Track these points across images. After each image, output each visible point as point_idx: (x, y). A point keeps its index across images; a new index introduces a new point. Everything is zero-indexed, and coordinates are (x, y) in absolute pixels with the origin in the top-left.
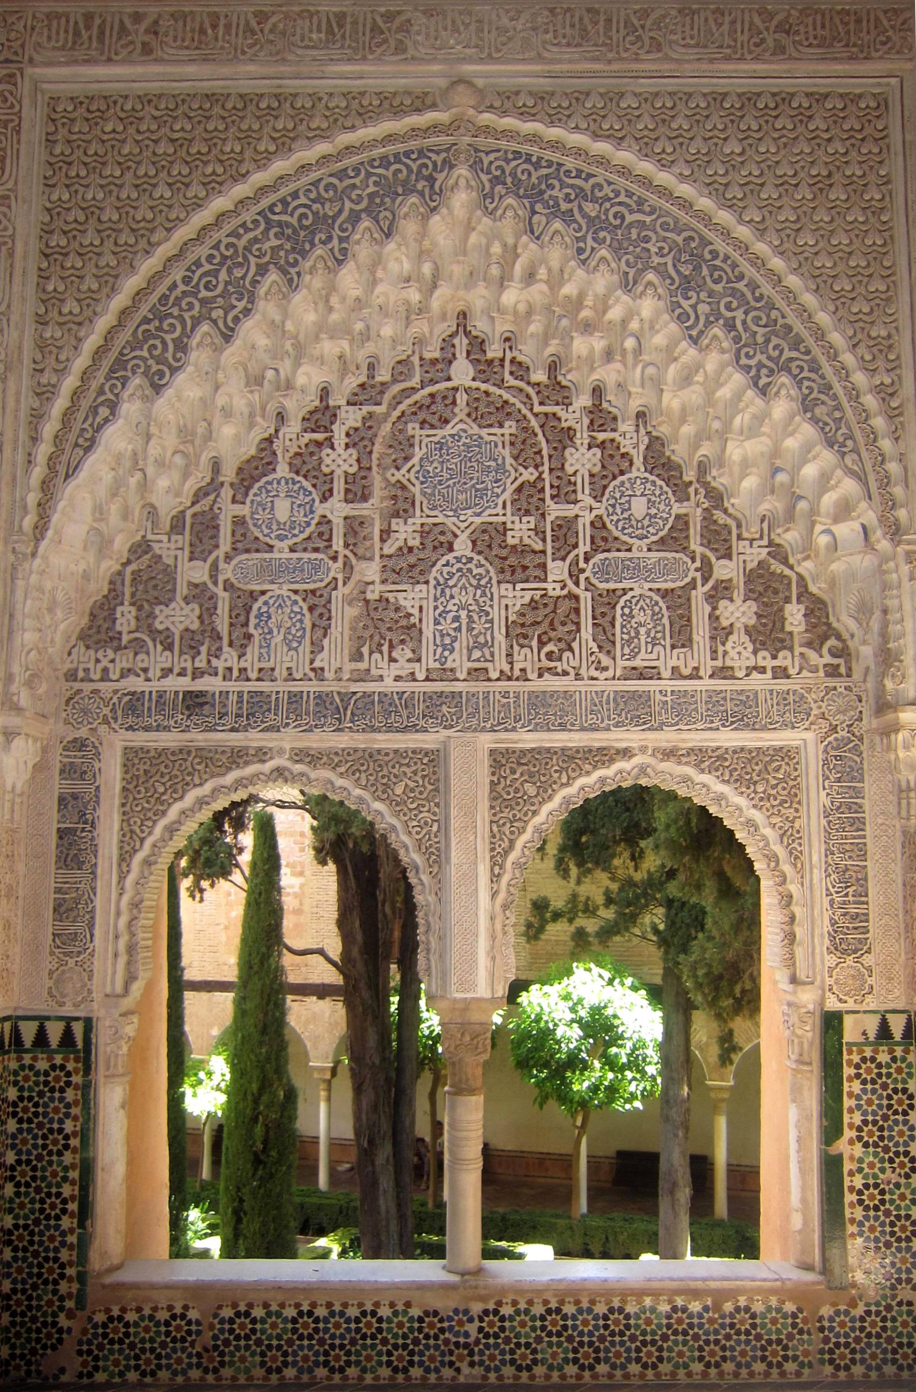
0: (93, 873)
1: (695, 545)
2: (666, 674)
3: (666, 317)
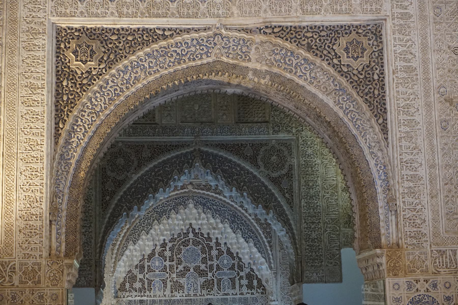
1: (236, 269)
2: (231, 294)
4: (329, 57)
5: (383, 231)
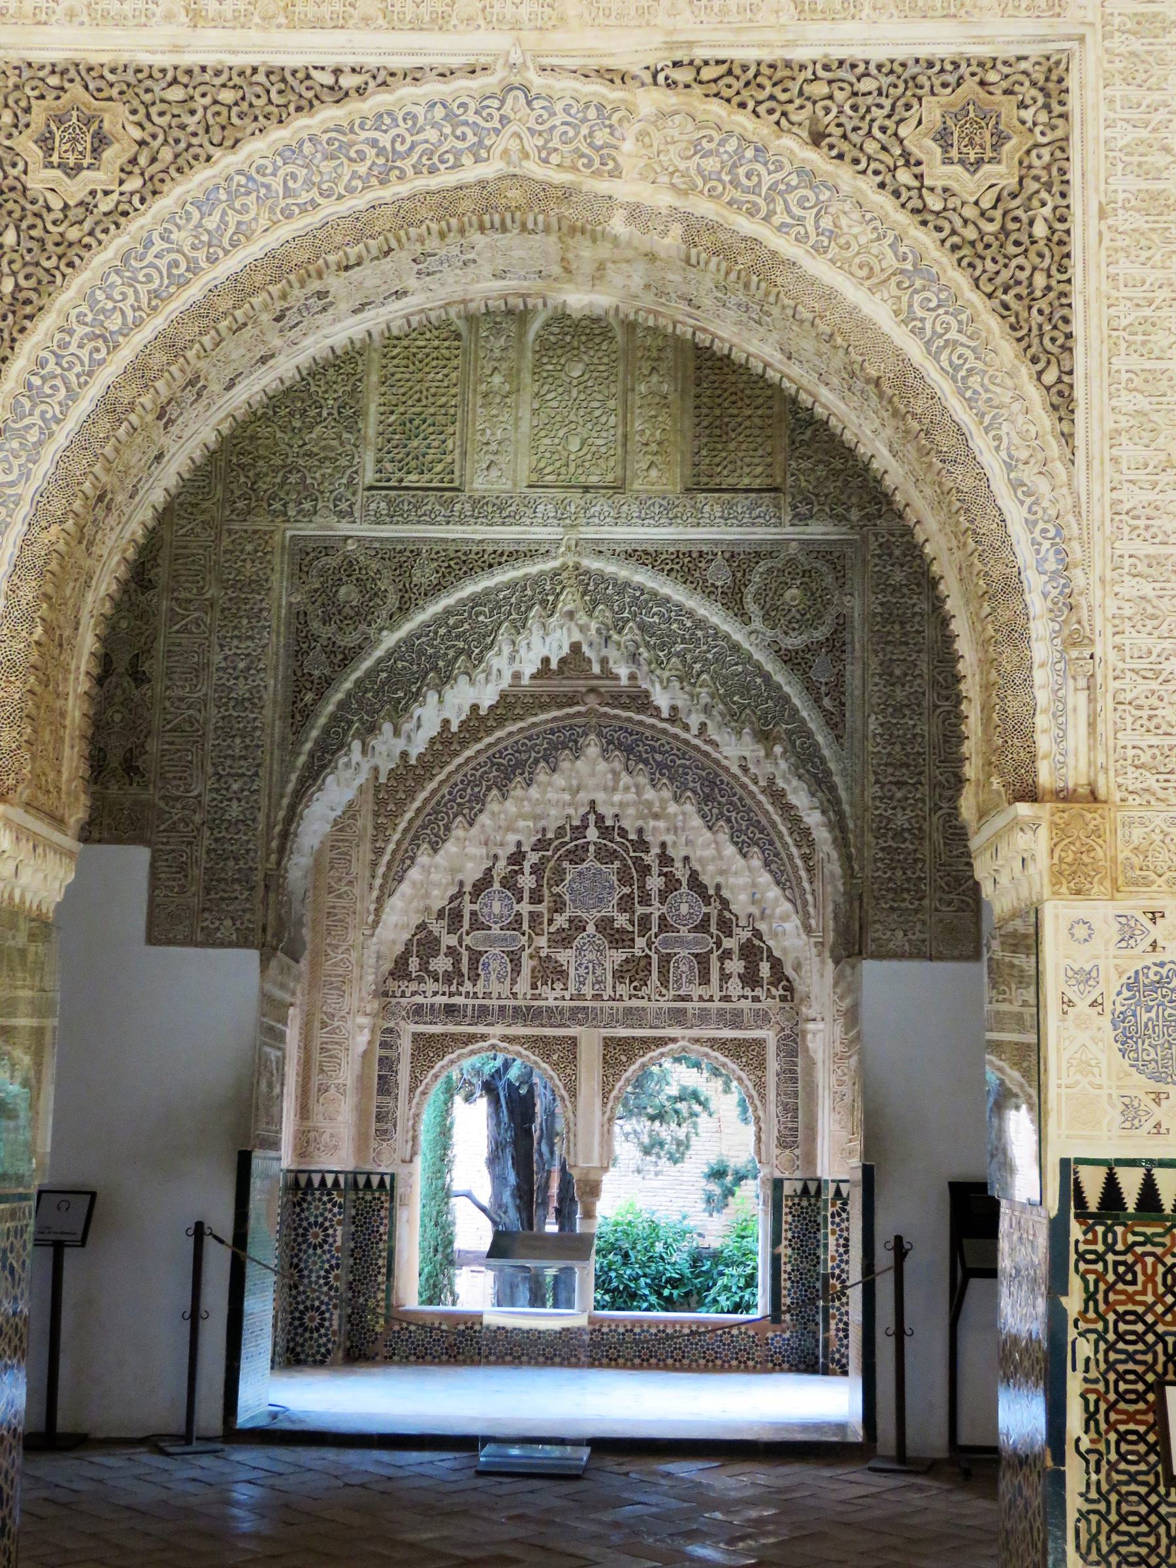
1: (713, 929)
2: (696, 998)
4: (882, 162)
5: (1043, 743)
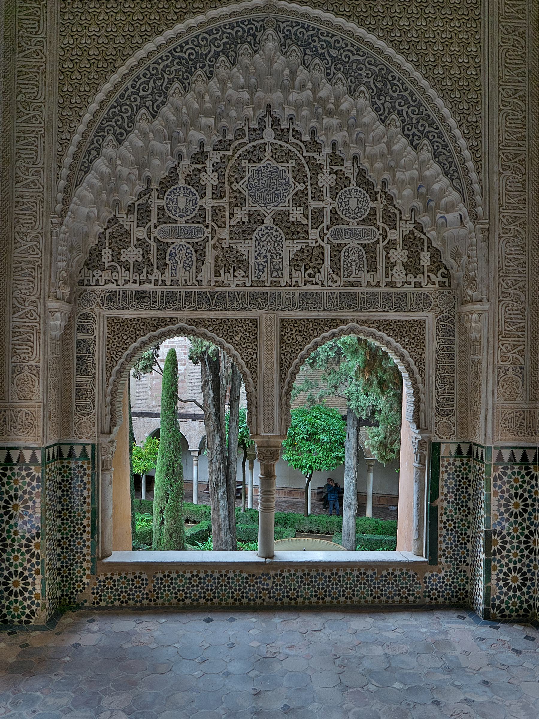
0: (94, 377)
3: (369, 109)
